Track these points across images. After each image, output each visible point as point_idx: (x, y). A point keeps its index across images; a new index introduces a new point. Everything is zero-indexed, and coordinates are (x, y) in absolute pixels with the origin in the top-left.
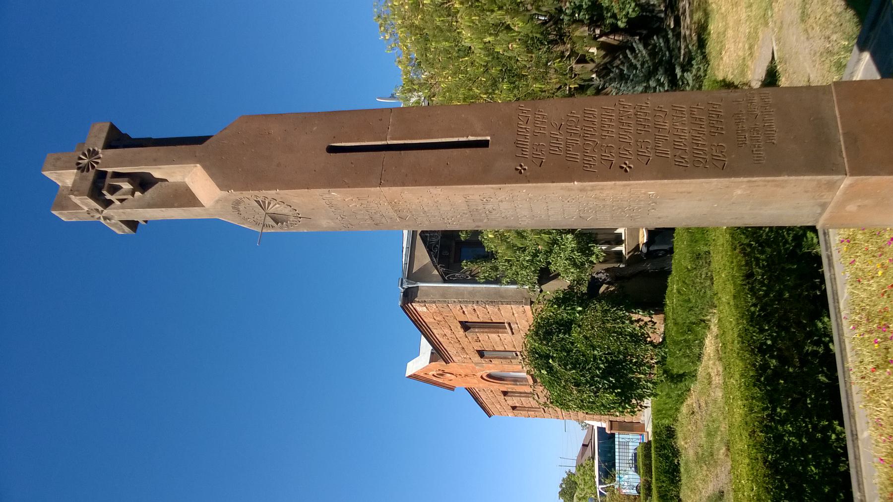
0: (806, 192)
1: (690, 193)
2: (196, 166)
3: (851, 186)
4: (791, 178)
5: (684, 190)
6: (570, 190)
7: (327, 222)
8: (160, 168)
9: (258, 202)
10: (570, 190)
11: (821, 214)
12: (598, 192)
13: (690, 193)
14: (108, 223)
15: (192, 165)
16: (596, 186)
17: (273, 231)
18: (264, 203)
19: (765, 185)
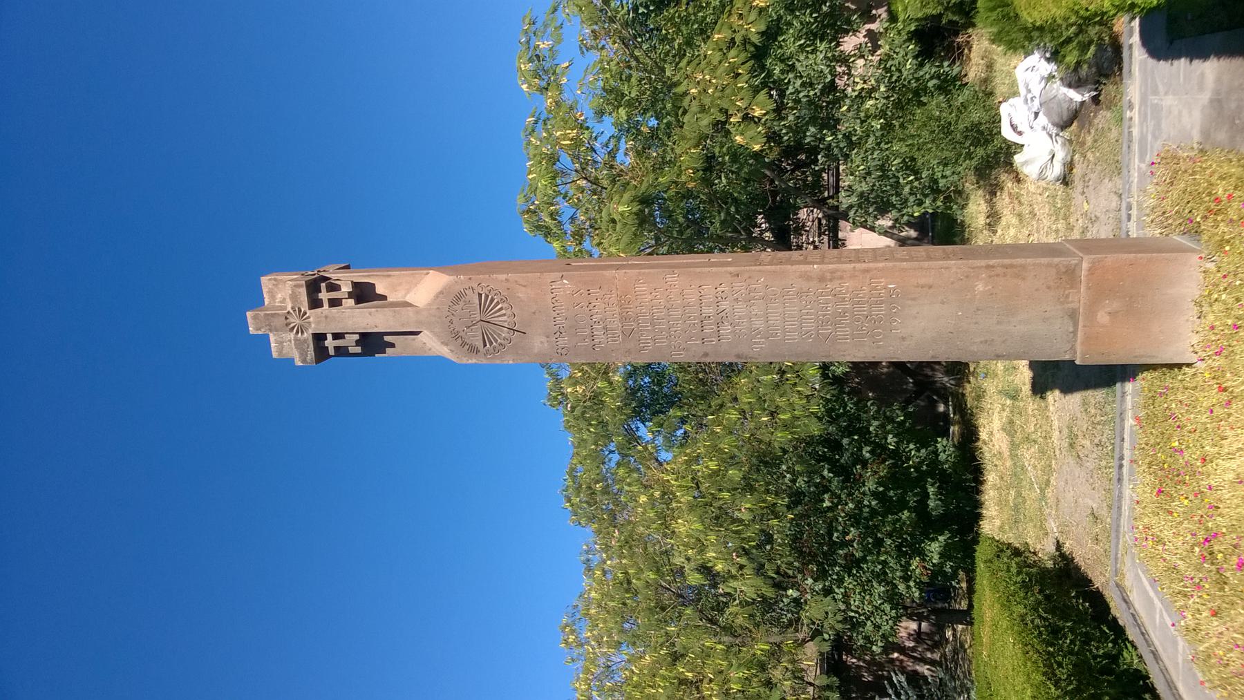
0: (1049, 288)
1: (930, 287)
2: (428, 274)
3: (1091, 271)
4: (1029, 260)
5: (922, 281)
6: (807, 277)
7: (542, 342)
8: (389, 276)
9: (480, 295)
10: (807, 277)
11: (1075, 332)
12: (836, 283)
13: (930, 287)
14: (296, 340)
15: (425, 272)
16: (837, 271)
17: (474, 361)
18: (487, 296)
19: (1005, 275)
